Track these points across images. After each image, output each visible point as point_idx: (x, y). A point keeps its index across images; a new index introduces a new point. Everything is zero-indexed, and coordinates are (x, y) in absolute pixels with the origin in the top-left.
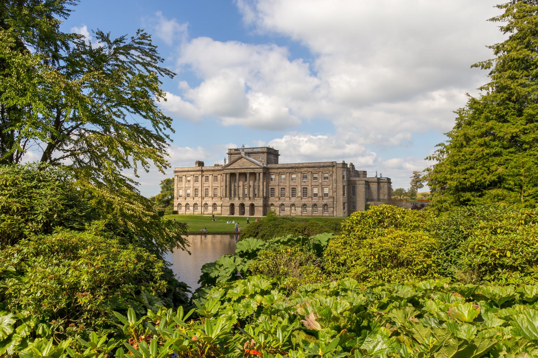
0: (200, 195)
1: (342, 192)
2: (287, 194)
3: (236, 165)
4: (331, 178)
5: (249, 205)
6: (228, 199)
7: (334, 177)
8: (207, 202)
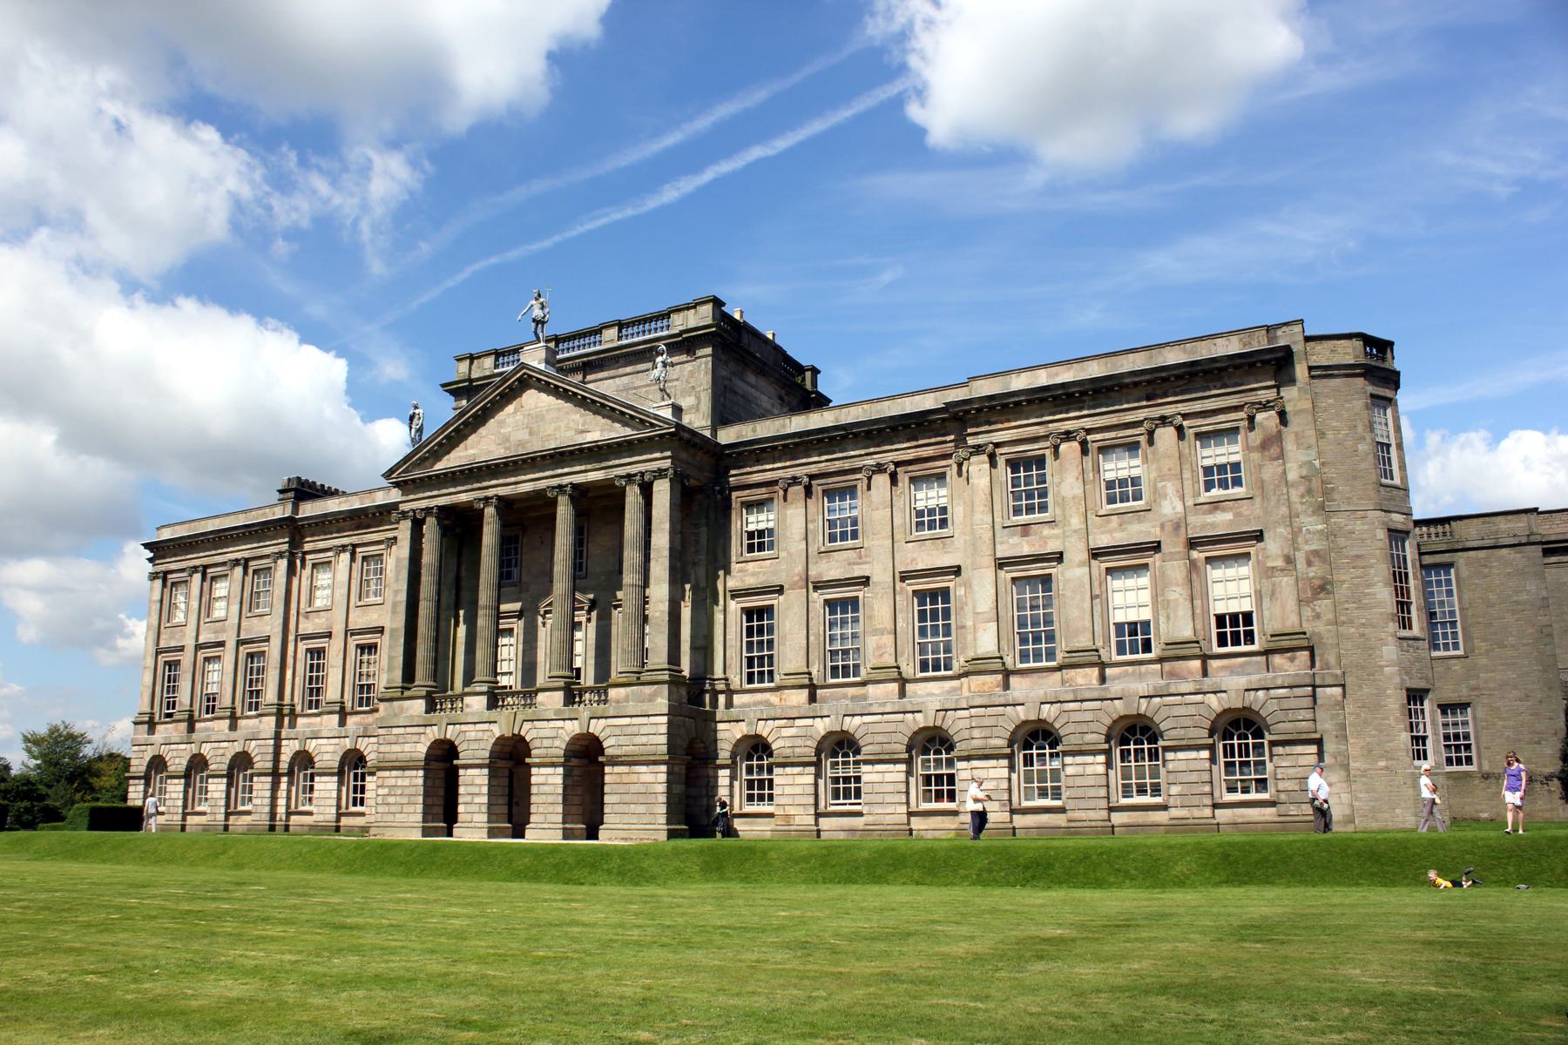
0: (270, 695)
1: (1384, 595)
2: (876, 649)
3: (481, 447)
4: (1270, 471)
5: (559, 747)
6: (420, 705)
7: (1297, 458)
8: (311, 746)
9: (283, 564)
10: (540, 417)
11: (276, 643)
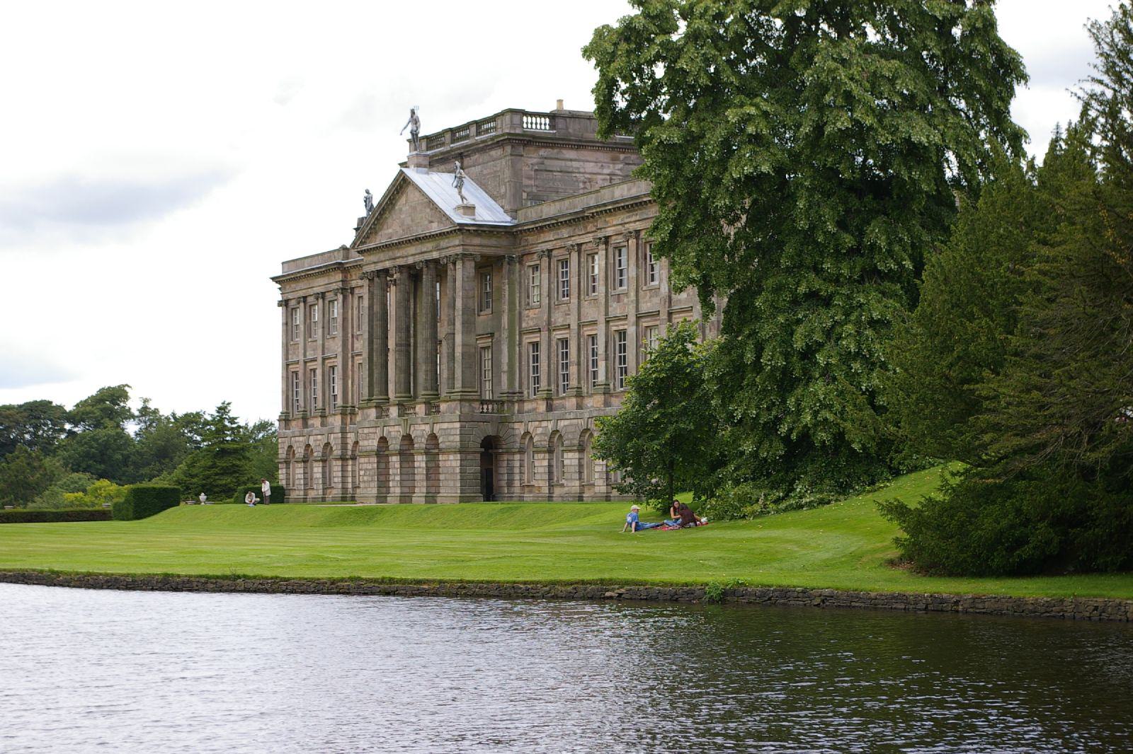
9: (340, 297)
11: (340, 359)
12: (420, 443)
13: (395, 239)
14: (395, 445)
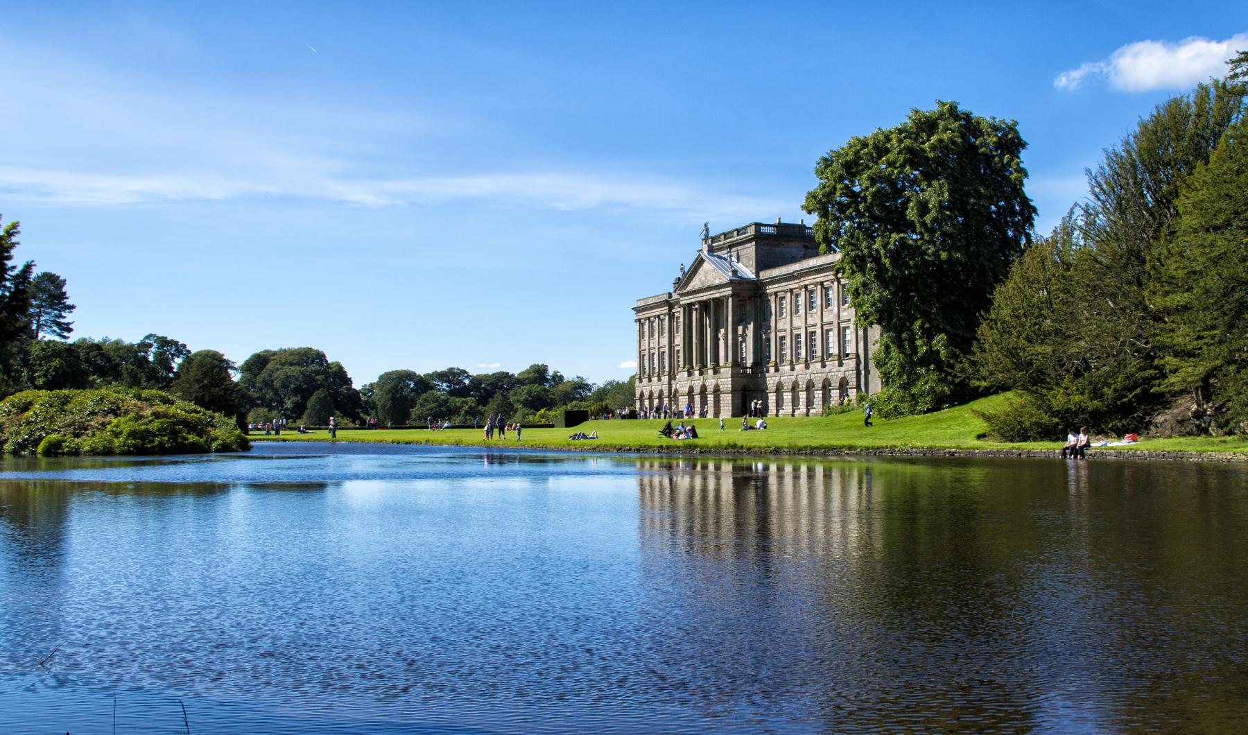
0: (667, 369)
10: (706, 273)
12: (710, 389)
13: (697, 287)
14: (697, 390)
